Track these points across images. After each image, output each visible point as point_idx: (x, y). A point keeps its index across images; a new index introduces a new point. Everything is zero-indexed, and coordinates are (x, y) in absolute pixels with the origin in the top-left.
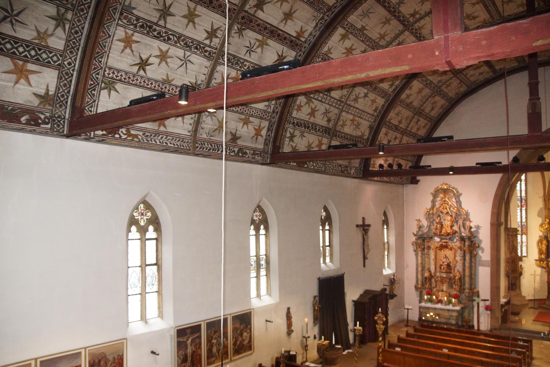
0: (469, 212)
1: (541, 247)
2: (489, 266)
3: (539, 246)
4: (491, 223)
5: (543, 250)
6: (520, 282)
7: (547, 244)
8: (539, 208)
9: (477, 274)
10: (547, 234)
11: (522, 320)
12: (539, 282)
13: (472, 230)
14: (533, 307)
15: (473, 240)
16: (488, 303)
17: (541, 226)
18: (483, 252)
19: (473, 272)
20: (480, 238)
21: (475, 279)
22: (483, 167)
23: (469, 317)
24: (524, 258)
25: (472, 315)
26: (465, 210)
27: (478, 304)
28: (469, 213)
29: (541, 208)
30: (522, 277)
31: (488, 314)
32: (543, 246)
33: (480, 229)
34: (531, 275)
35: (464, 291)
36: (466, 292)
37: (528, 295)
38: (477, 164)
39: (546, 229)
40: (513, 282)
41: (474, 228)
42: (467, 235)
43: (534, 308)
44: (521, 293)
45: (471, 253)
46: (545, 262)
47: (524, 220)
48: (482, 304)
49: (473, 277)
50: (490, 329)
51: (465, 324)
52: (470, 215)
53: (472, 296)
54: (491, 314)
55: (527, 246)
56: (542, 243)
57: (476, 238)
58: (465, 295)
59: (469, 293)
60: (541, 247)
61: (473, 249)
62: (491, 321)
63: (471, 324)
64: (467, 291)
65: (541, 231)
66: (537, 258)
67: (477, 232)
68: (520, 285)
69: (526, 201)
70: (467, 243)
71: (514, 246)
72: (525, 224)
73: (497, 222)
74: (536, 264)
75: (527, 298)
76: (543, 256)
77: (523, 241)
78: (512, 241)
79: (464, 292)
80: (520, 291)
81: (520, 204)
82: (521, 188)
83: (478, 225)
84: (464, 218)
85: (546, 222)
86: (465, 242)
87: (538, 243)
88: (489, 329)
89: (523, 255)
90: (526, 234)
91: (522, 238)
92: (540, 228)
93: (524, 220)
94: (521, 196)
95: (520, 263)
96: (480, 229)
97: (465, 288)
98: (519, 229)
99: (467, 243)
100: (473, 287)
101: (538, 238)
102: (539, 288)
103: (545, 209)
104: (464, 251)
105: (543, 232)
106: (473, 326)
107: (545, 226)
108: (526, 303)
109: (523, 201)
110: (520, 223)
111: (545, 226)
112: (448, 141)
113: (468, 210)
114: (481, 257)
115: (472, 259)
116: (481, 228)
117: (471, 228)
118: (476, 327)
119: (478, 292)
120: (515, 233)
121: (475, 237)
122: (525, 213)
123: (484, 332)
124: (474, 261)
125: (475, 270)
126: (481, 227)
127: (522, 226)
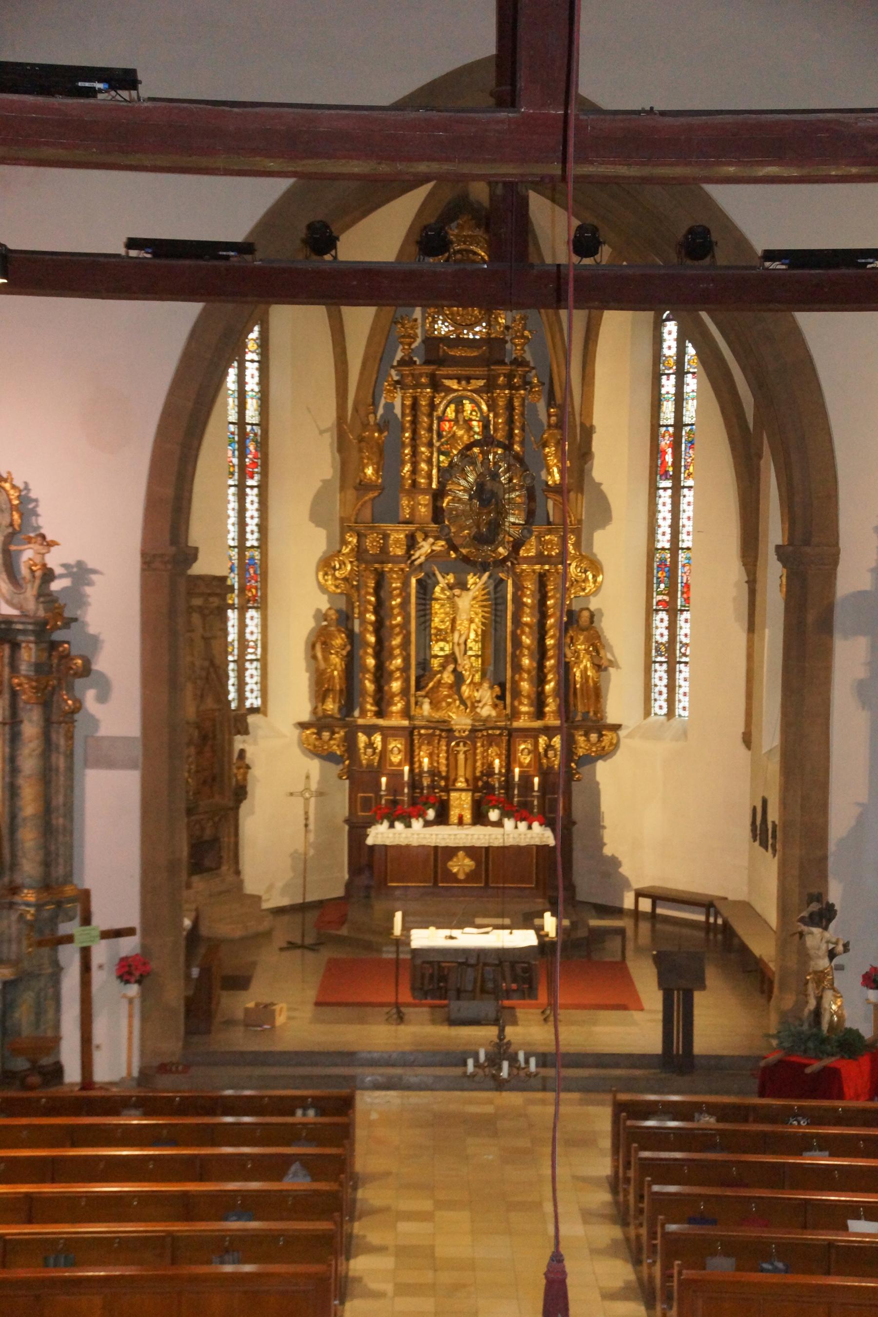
0: (33, 495)
1: (322, 665)
2: (134, 767)
3: (314, 657)
4: (144, 554)
5: (332, 677)
6: (236, 834)
7: (348, 648)
8: (320, 484)
9: (76, 803)
10: (350, 604)
11: (277, 1008)
13: (56, 586)
14: (298, 941)
15: (57, 636)
16: (129, 946)
17: (326, 564)
18: (103, 698)
19: (59, 800)
20: (92, 630)
21: (69, 831)
22: (158, 261)
23: (37, 1024)
24: (251, 719)
25: (50, 1015)
26: (14, 487)
27: (86, 954)
28: (36, 500)
29: (324, 481)
30: (244, 807)
31: (131, 1001)
32: (335, 659)
33: (90, 583)
34: (291, 794)
35: (17, 899)
36: (28, 904)
37: (271, 887)
38: (132, 243)
39: (346, 579)
40: (208, 834)
41: (62, 576)
42: (24, 615)
43: (302, 947)
44: (240, 884)
45: (47, 704)
46: (341, 734)
47: (252, 540)
48: (101, 953)
49: (59, 821)
50: (142, 1072)
51: (21, 1064)
52: (39, 510)
53: (53, 921)
54: (144, 996)
55: (263, 661)
56: (327, 647)
57: (73, 625)
58: (21, 917)
59: (39, 906)
60: (322, 665)
61: (59, 683)
62: (143, 1030)
63: (45, 1061)
64: (30, 896)
65: (323, 589)
66: (306, 717)
67: (76, 594)
68: (236, 844)
69: (263, 445)
70: (28, 654)
71: (212, 663)
72: (257, 554)
73: (172, 550)
74: (301, 743)
75: (265, 905)
76: (331, 706)
77: (248, 636)
78: (204, 638)
79: (11, 905)
80: (238, 872)
81: (235, 461)
82: (241, 380)
83: (80, 564)
84: (11, 525)
85: (345, 550)
86: (15, 646)
87: (313, 646)
88: (135, 1073)
89: (248, 704)
90: (262, 605)
91: (242, 626)
92: (321, 574)
93: (252, 540)
94: (241, 422)
95: (239, 743)
96: (90, 583)
97: (19, 880)
98: (234, 580)
99: (28, 654)
100: (59, 871)
101: (311, 624)
102: (311, 852)
103: (342, 488)
104: (14, 695)
105: (332, 596)
106: (58, 1070)
107: (342, 563)
108: (266, 925)
109: (252, 447)
110: (234, 553)
111: (342, 563)
112: (106, 96)
113: (27, 487)
114: (94, 722)
115: (54, 736)
116: (94, 577)
117: (48, 575)
118: (72, 1074)
119: (86, 895)
120: (215, 601)
121: (69, 622)
123: (115, 1090)
124: (62, 742)
125: (70, 787)
126: (95, 572)
127: (243, 566)
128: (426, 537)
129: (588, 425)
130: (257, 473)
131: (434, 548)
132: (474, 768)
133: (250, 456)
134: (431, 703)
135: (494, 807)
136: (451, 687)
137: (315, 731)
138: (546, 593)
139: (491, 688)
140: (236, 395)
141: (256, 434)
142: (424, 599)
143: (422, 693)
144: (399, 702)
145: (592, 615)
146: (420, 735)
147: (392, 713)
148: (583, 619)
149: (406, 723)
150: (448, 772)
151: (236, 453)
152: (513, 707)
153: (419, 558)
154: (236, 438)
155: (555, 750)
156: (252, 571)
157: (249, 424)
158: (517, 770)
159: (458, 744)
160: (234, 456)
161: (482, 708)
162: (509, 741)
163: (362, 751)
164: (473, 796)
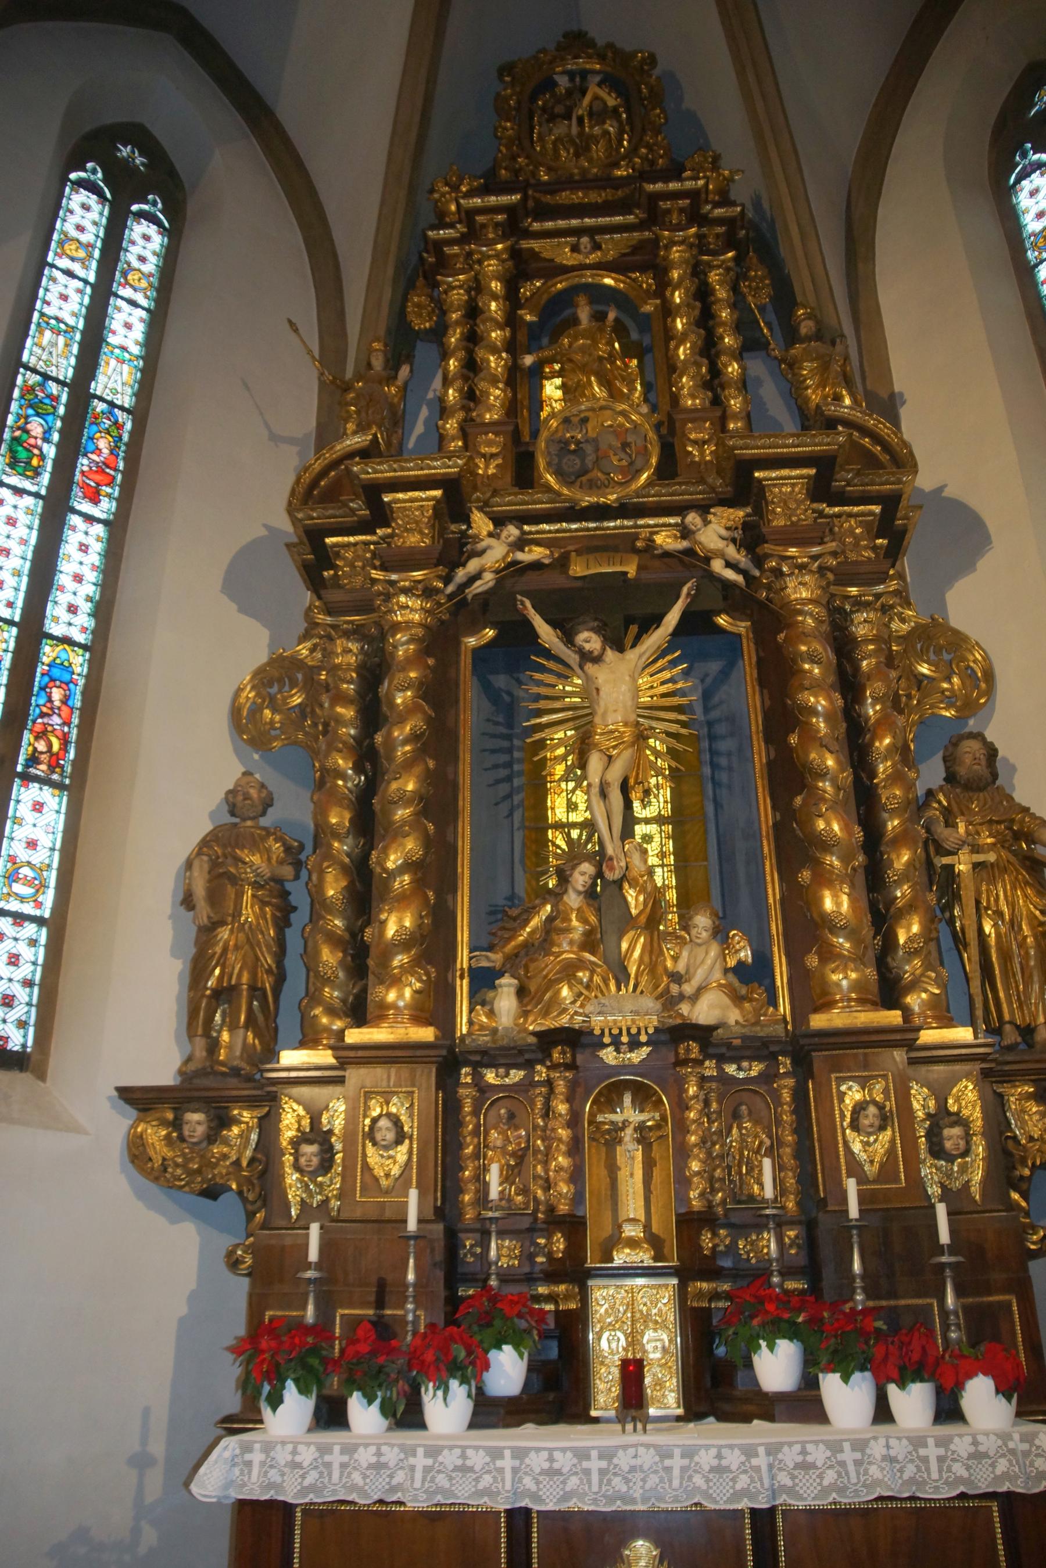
12: (158, 1448)
72: (79, 661)
122: (94, 557)
128: (499, 521)
129: (884, 394)
130: (109, 496)
131: (520, 556)
132: (683, 1182)
133: (94, 457)
134: (521, 992)
135: (776, 1329)
136: (589, 943)
137: (170, 1116)
138: (857, 668)
139: (720, 933)
140: (78, 337)
141: (119, 426)
142: (509, 738)
143: (496, 958)
144: (407, 970)
145: (992, 753)
146: (482, 1089)
147: (383, 1006)
148: (968, 760)
149: (426, 1034)
150: (578, 1198)
151: (56, 437)
152: (800, 978)
153: (477, 576)
154: (62, 410)
155: (964, 1123)
156: (57, 695)
157: (101, 399)
158: (851, 1186)
159: (610, 1098)
160: (45, 439)
161: (694, 998)
162: (800, 1096)
163: (288, 1159)
164: (682, 1293)
